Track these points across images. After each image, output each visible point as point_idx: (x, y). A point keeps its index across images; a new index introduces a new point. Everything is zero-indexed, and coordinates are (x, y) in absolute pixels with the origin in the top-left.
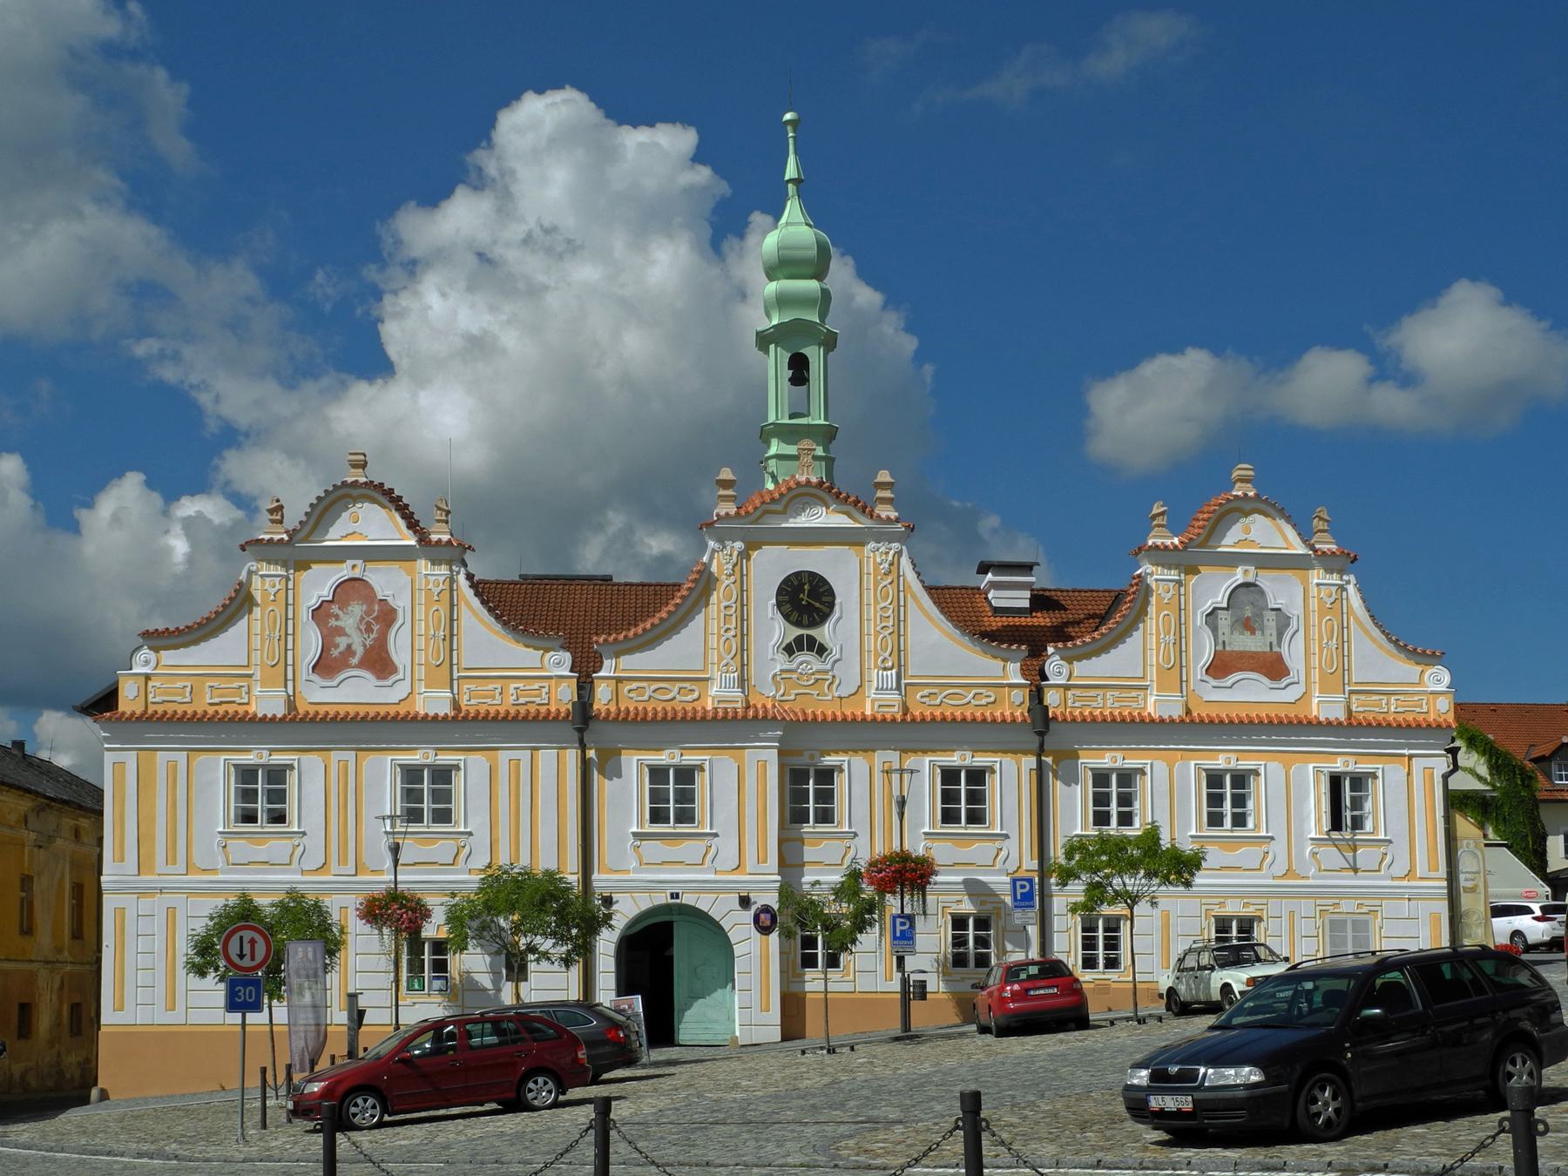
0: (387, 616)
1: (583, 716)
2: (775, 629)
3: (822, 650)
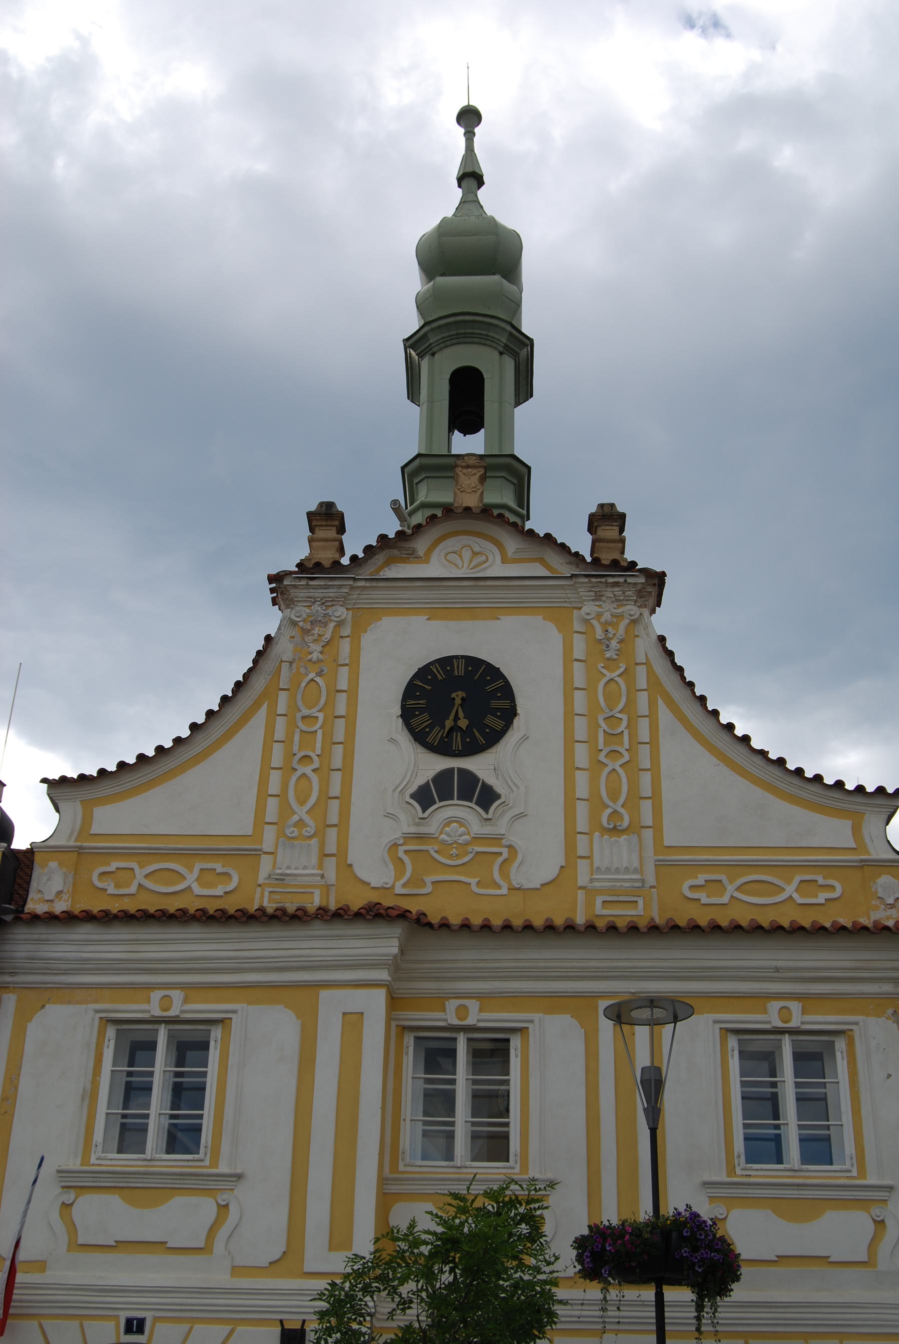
3: (487, 797)
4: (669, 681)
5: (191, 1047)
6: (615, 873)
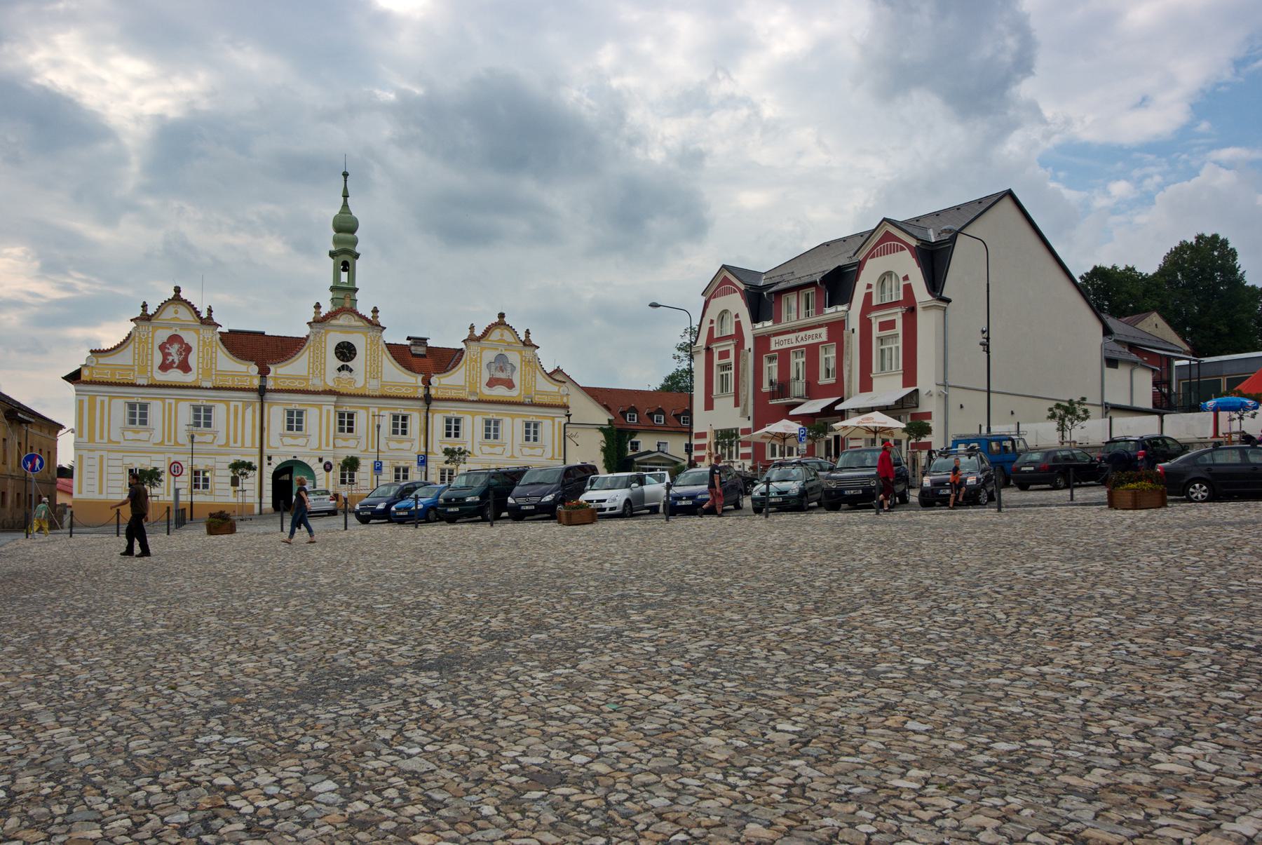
0: (188, 349)
2: (334, 362)
3: (351, 370)
5: (300, 413)
6: (373, 387)
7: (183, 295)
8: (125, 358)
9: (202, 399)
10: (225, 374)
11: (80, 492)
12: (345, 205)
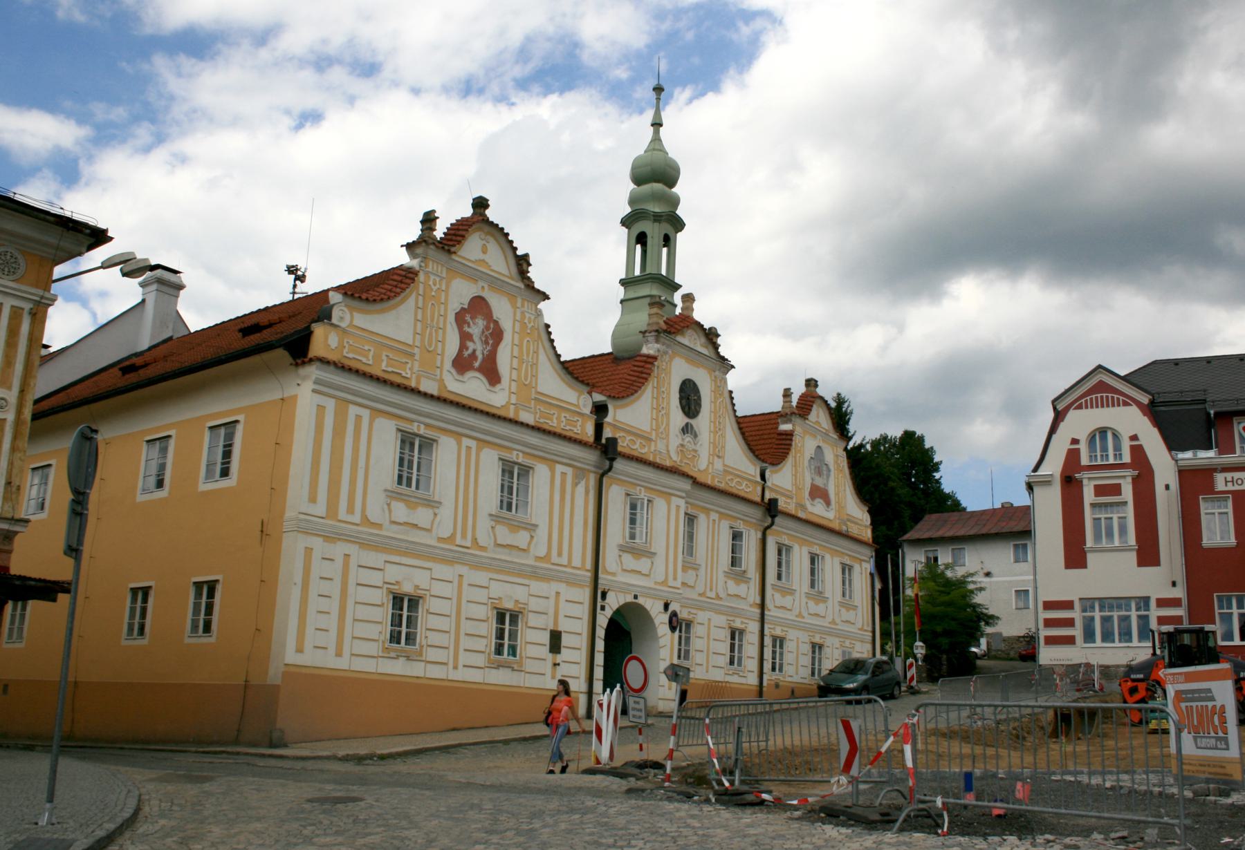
0: (496, 335)
1: (608, 450)
4: (730, 407)
7: (490, 214)
8: (395, 323)
9: (521, 447)
10: (543, 400)
11: (300, 650)
12: (656, 138)
